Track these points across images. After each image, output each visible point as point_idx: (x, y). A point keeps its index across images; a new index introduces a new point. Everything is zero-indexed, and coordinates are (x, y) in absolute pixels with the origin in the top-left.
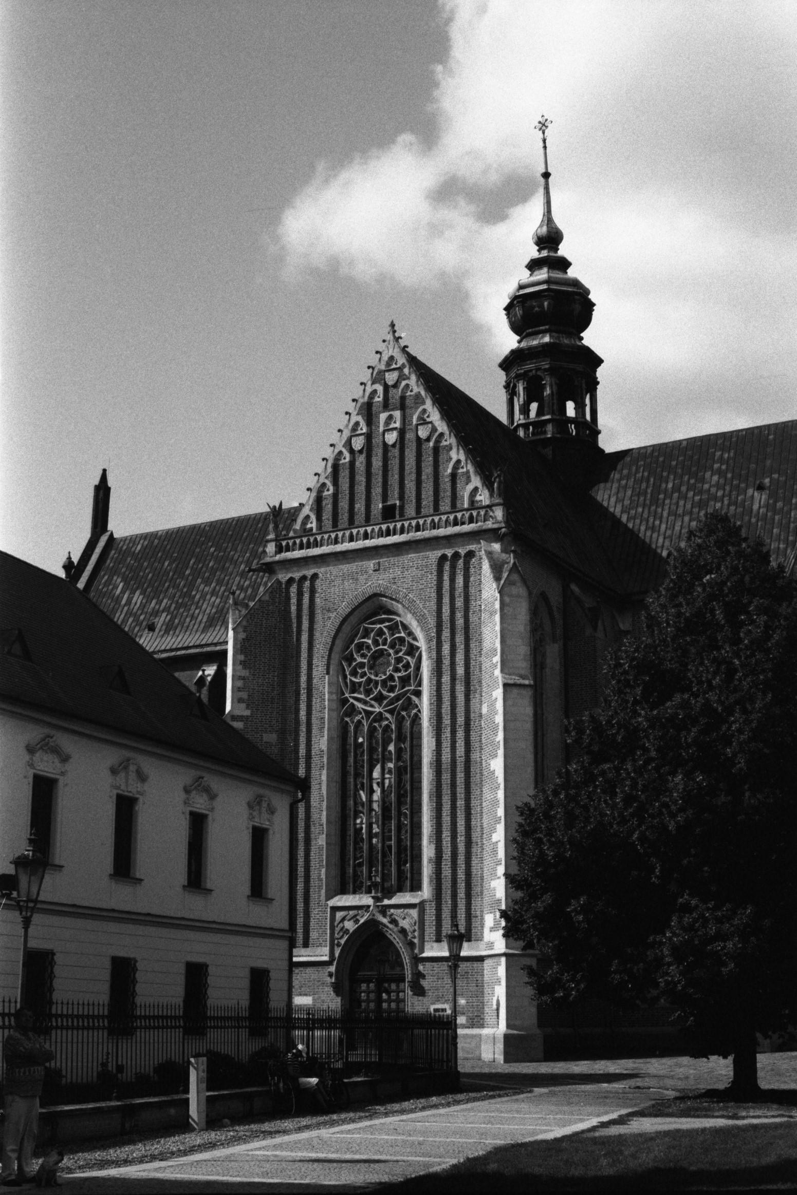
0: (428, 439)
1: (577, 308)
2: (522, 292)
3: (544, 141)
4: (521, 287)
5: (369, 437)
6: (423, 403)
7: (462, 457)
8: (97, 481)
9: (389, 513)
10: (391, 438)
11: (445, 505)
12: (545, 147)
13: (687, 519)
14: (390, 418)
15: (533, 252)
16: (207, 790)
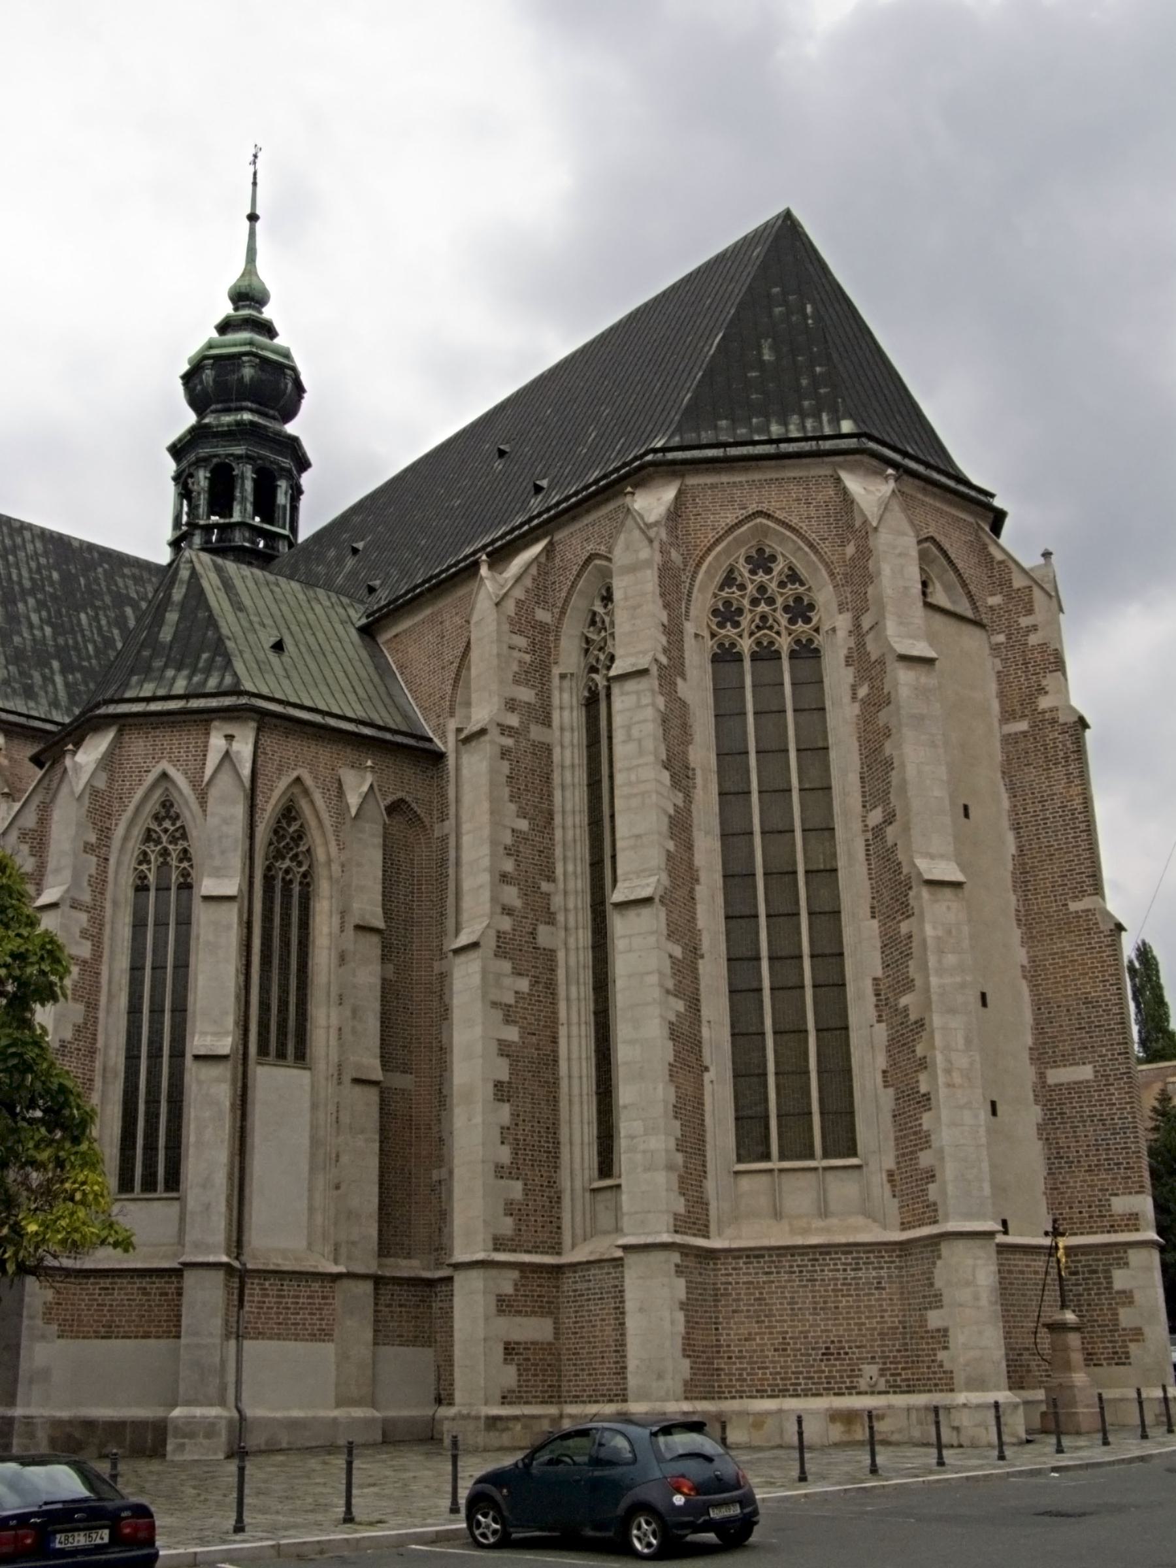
3: (255, 174)
12: (255, 184)
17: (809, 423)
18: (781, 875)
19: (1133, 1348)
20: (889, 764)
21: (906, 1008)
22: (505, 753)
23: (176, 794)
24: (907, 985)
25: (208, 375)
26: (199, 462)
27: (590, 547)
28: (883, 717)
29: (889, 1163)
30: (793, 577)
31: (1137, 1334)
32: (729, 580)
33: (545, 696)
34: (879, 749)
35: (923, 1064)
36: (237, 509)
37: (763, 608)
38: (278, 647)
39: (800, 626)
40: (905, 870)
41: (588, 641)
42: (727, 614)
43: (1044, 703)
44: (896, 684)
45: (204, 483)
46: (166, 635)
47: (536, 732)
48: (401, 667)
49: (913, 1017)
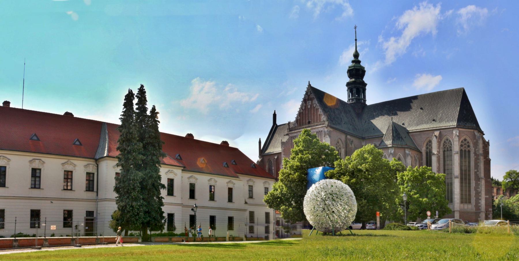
0: (315, 107)
5: (305, 106)
9: (309, 123)
10: (309, 107)
11: (318, 121)
18: (465, 175)
20: (479, 166)
21: (478, 191)
22: (437, 157)
24: (479, 188)
28: (478, 161)
29: (474, 204)
30: (468, 142)
32: (462, 142)
33: (439, 150)
35: (480, 196)
37: (465, 145)
39: (469, 148)
40: (480, 177)
41: (444, 144)
42: (461, 146)
43: (487, 158)
44: (480, 158)
47: (439, 155)
48: (414, 140)
49: (479, 191)
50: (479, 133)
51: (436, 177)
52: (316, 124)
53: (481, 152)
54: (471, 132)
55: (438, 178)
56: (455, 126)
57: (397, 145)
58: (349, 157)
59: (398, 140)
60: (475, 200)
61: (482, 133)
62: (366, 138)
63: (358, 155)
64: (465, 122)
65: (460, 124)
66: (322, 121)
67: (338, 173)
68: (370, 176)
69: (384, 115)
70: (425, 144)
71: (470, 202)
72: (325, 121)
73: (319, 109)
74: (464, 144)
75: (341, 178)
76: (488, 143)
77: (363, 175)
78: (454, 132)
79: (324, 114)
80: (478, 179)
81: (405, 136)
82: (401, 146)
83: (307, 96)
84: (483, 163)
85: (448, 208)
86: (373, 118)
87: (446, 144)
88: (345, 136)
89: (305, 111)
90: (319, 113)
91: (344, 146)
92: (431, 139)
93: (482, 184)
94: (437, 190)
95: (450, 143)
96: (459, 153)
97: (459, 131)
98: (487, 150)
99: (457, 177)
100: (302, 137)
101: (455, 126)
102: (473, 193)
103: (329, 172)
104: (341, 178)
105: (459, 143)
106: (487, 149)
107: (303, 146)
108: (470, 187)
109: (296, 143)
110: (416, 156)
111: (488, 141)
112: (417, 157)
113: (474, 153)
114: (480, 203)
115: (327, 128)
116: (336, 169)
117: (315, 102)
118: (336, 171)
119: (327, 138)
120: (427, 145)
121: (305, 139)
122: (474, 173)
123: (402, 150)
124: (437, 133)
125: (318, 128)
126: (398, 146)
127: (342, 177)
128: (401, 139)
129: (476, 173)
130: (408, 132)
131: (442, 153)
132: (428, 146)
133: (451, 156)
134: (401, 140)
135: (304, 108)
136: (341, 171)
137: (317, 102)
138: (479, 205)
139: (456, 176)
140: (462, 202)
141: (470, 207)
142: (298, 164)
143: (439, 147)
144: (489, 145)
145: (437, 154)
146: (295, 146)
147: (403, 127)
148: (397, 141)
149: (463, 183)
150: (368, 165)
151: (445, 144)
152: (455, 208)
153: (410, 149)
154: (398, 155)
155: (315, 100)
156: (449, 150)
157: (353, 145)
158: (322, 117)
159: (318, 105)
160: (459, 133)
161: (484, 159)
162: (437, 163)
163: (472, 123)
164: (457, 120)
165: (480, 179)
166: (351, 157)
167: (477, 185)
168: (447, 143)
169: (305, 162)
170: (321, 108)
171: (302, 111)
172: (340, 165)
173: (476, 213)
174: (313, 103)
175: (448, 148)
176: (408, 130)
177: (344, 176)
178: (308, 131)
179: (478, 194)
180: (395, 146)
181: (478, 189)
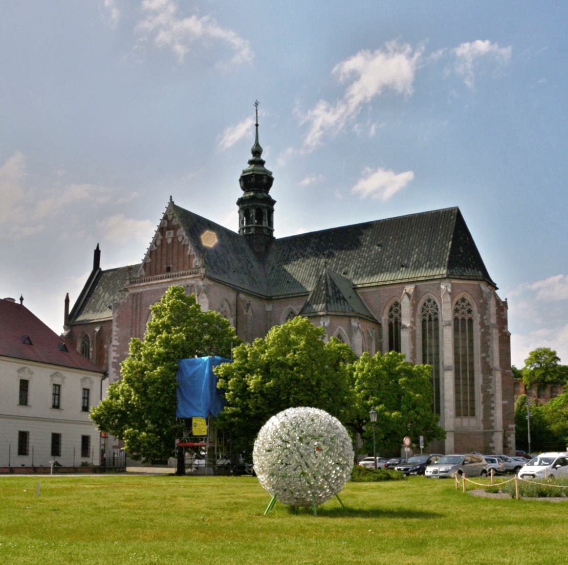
0: (181, 242)
1: (265, 181)
2: (246, 174)
4: (244, 172)
5: (162, 241)
6: (180, 228)
7: (192, 249)
8: (95, 248)
10: (169, 241)
11: (187, 267)
13: (297, 266)
14: (169, 233)
15: (251, 157)
16: (61, 376)
17: (473, 271)
18: (465, 363)
19: (510, 451)
20: (488, 347)
21: (488, 392)
22: (411, 333)
23: (341, 333)
24: (491, 388)
25: (253, 180)
26: (253, 207)
27: (427, 290)
28: (488, 337)
29: (482, 417)
30: (469, 304)
31: (511, 448)
32: (457, 303)
33: (415, 319)
34: (486, 343)
35: (493, 402)
36: (264, 223)
37: (463, 310)
38: (350, 297)
39: (470, 315)
42: (456, 311)
43: (504, 331)
45: (254, 214)
46: (331, 294)
47: (414, 328)
48: (364, 299)
49: (491, 393)
50: (489, 287)
51: (415, 371)
52: (182, 272)
53: (493, 320)
54: (473, 285)
55: (418, 374)
56: (445, 276)
57: (335, 311)
58: (261, 339)
59: (337, 302)
60: (484, 410)
61: (494, 286)
62: (274, 298)
63: (279, 336)
64: (463, 268)
65: (454, 271)
66: (194, 267)
67: (239, 369)
68: (302, 376)
69: (308, 258)
70: (387, 309)
71: (473, 414)
72: (199, 268)
73: (188, 245)
74: (460, 307)
75: (246, 379)
76: (505, 303)
77: (289, 374)
78: (443, 287)
79: (199, 255)
80: (488, 370)
81: (349, 296)
82: (342, 314)
83: (166, 221)
84: (497, 341)
85: (440, 429)
86: (287, 261)
87: (427, 309)
88: (235, 294)
89: (162, 248)
90: (188, 254)
91: (234, 313)
92: (398, 300)
93: (497, 379)
94: (419, 397)
95: (434, 306)
96: (452, 323)
97: (453, 285)
98: (503, 317)
99: (448, 369)
100: (168, 301)
101: (445, 276)
102: (479, 396)
103: (223, 366)
104: (246, 379)
105: (452, 305)
106: (503, 315)
107: (170, 318)
108: (472, 385)
109: (156, 311)
110: (369, 331)
111: (505, 300)
112: (372, 332)
113: (480, 324)
114: (492, 415)
115: (203, 279)
116: (236, 361)
117: (182, 232)
118: (235, 365)
119: (203, 298)
120: (391, 309)
121: (174, 304)
122: (480, 362)
123: (345, 321)
124: (410, 289)
125: (185, 279)
126: (339, 314)
127: (248, 377)
128: (342, 301)
129: (483, 359)
130: (355, 288)
131: (419, 324)
132: (393, 312)
133: (437, 329)
134: (342, 303)
135: (158, 243)
136: (246, 365)
137: (184, 233)
138: (491, 418)
139: (448, 367)
140: (458, 414)
141: (474, 424)
142: (161, 350)
143: (414, 315)
144: (507, 308)
145: (411, 327)
146: (154, 316)
147: (345, 278)
148: (335, 303)
149: (460, 379)
150: (299, 354)
151: (425, 307)
152: (446, 427)
153: (360, 318)
154: (337, 329)
155: (182, 229)
156: (433, 318)
157: (250, 310)
158: (194, 260)
159: (186, 238)
160: (452, 289)
161: (499, 333)
162: (411, 344)
163: (475, 269)
164: (446, 264)
165: (492, 370)
166: (264, 338)
167: (487, 383)
168: (429, 306)
169: (175, 347)
170: (192, 245)
171: (155, 248)
172: (244, 355)
173: (485, 433)
174: (178, 234)
175: (430, 315)
176: (355, 283)
177: (252, 375)
178: (179, 290)
179: (488, 398)
180: (331, 313)
181: (488, 390)
